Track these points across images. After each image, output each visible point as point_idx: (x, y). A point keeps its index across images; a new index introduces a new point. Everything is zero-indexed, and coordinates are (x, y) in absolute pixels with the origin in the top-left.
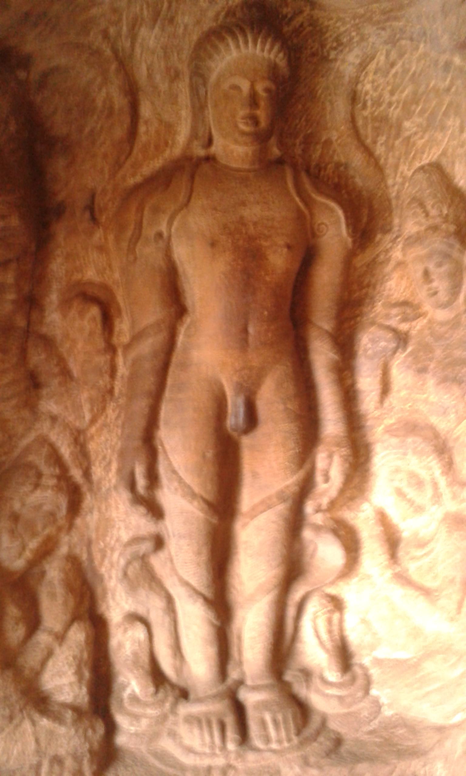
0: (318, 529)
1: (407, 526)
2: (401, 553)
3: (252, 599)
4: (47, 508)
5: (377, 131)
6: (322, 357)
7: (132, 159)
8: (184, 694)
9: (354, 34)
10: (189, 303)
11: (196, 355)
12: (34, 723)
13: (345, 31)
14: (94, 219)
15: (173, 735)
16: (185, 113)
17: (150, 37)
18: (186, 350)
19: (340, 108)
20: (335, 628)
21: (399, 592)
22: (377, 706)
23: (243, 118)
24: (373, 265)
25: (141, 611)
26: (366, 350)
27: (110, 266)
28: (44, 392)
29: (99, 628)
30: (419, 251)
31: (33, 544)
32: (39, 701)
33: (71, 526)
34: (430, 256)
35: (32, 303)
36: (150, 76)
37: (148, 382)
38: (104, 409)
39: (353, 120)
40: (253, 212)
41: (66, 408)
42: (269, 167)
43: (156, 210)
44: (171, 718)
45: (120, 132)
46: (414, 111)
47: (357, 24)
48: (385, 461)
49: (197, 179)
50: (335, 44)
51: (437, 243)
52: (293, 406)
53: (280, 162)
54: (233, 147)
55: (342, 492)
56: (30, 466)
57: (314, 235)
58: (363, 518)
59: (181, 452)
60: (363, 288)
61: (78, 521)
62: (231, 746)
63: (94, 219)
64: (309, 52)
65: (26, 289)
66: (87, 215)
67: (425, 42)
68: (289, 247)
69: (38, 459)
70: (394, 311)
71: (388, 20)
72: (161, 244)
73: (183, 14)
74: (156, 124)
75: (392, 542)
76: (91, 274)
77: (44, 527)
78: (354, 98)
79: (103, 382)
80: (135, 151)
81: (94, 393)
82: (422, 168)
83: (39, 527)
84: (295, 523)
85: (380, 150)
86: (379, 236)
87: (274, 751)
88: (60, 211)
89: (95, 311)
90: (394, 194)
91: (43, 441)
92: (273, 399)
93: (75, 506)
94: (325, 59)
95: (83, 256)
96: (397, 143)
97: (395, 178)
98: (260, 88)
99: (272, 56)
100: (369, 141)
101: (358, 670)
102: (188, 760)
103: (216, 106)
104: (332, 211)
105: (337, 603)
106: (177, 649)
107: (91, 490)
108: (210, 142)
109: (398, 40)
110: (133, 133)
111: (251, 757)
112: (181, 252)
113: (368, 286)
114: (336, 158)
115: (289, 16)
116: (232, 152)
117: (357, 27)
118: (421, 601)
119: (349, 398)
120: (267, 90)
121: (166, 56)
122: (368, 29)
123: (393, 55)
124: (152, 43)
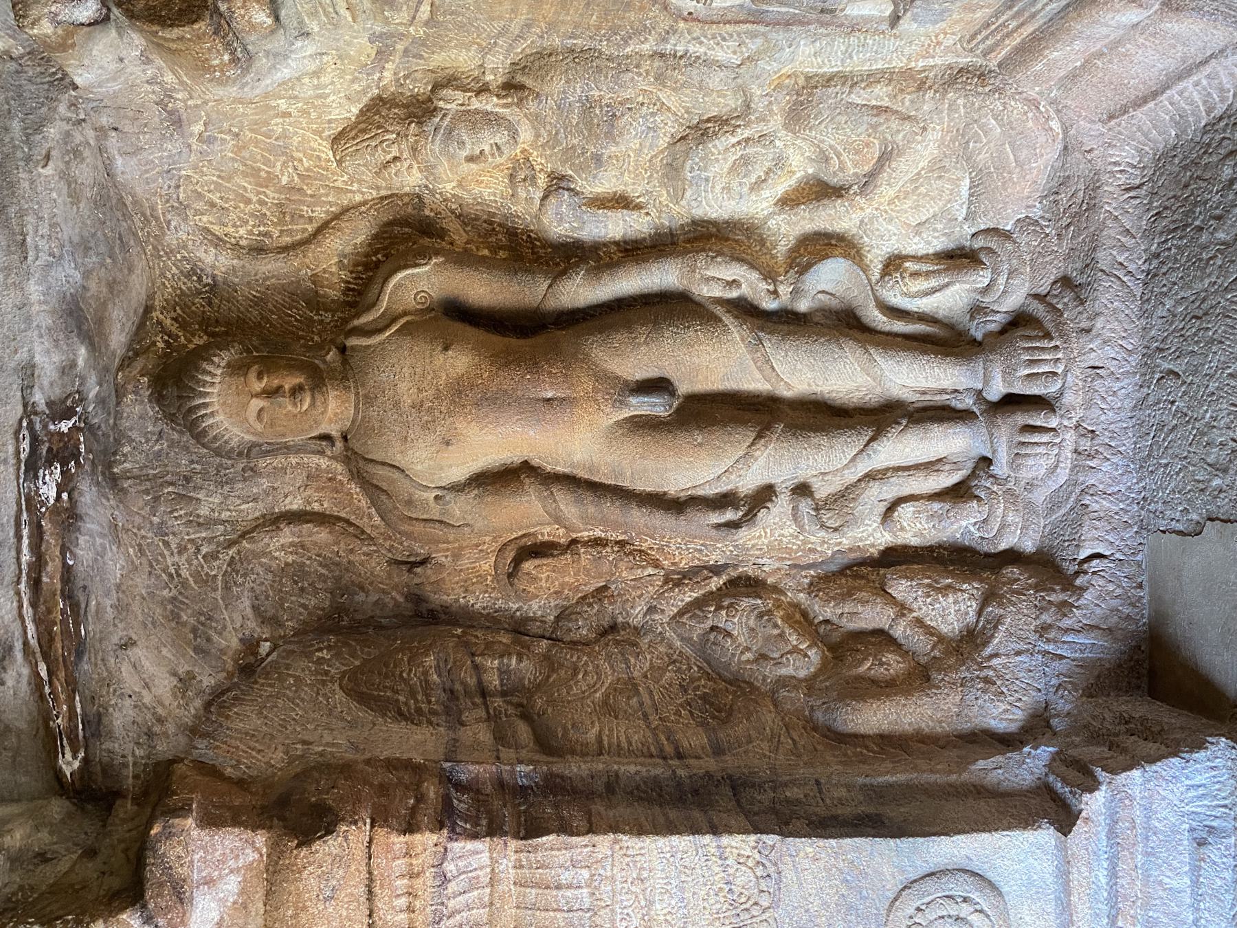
0: (796, 293)
1: (800, 165)
2: (834, 181)
3: (878, 379)
4: (752, 623)
5: (297, 217)
6: (580, 291)
7: (353, 518)
8: (986, 461)
9: (179, 257)
10: (517, 460)
11: (578, 457)
12: (996, 655)
13: (178, 268)
14: (423, 562)
15: (1030, 486)
16: (294, 460)
17: (208, 503)
18: (572, 465)
19: (270, 267)
20: (925, 268)
21: (885, 191)
22: (1027, 223)
23: (295, 404)
24: (464, 218)
25: (882, 508)
26: (573, 229)
27: (477, 546)
28: (620, 619)
30: (444, 168)
31: (793, 639)
32: (971, 641)
33: (775, 589)
34: (451, 157)
35: (520, 628)
36: (255, 500)
37: (611, 509)
38: (640, 551)
39: (285, 249)
41: (639, 597)
43: (409, 503)
44: (1010, 485)
45: (322, 535)
46: (268, 172)
47: (166, 253)
48: (714, 204)
49: (370, 457)
50: (195, 278)
52: (642, 332)
53: (343, 350)
54: (330, 413)
55: (752, 266)
56: (704, 637)
57: (430, 309)
58: (787, 229)
60: (494, 229)
61: (770, 581)
62: (1053, 422)
63: (423, 562)
64: (207, 308)
65: (505, 639)
66: (418, 570)
67: (179, 169)
68: (446, 349)
70: (522, 194)
71: (157, 219)
72: (449, 497)
73: (179, 465)
74: (309, 492)
75: (822, 191)
76: (486, 566)
77: (776, 626)
78: (258, 250)
80: (343, 515)
81: (622, 565)
82: (340, 162)
83: (776, 632)
85: (320, 213)
86: (427, 212)
87: (1066, 371)
88: (416, 598)
89: (528, 566)
90: (374, 193)
92: (635, 358)
94: (214, 287)
95: (469, 577)
96: (309, 192)
97: (354, 192)
98: (258, 386)
99: (219, 372)
100: (310, 228)
101: (978, 244)
102: (1063, 475)
103: (284, 435)
104: (398, 286)
105: (894, 264)
107: (735, 566)
108: (326, 437)
109: (181, 203)
111: (1068, 398)
112: (459, 473)
113: (491, 223)
114: (334, 269)
115: (166, 338)
116: (336, 414)
117: (170, 253)
119: (634, 251)
120: (260, 377)
121: (230, 482)
122: (171, 239)
123: (200, 205)
124: (216, 499)
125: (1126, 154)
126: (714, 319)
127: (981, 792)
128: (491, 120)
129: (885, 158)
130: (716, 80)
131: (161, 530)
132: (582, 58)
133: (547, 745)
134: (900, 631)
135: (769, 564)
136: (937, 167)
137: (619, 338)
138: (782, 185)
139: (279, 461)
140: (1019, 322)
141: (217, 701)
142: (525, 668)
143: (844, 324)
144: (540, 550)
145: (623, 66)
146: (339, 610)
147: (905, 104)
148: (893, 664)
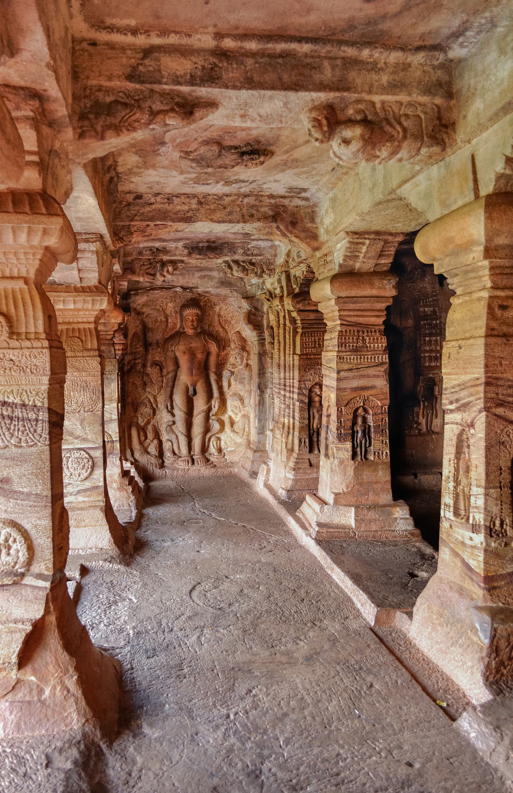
6: (213, 378)
11: (181, 377)
17: (171, 305)
21: (231, 434)
29: (160, 443)
35: (144, 366)
37: (170, 384)
40: (193, 345)
42: (198, 335)
43: (172, 345)
45: (164, 326)
48: (229, 403)
51: (237, 351)
53: (201, 332)
58: (225, 418)
59: (179, 400)
69: (146, 402)
75: (232, 423)
78: (219, 316)
79: (160, 384)
84: (207, 418)
88: (151, 344)
91: (147, 397)
93: (154, 413)
105: (219, 439)
106: (179, 448)
110: (167, 326)
112: (178, 354)
118: (236, 435)
125: (236, 470)
126: (208, 403)
127: (125, 450)
128: (242, 361)
129: (237, 433)
130: (248, 400)
131: (166, 298)
132: (251, 377)
133: (129, 371)
134: (148, 441)
135: (158, 417)
136: (236, 443)
137: (204, 385)
138: (233, 416)
139: (179, 318)
140: (208, 460)
141: (135, 309)
142: (139, 367)
143: (207, 429)
144: (161, 370)
145: (250, 384)
146: (148, 329)
147: (245, 434)
148: (143, 438)
